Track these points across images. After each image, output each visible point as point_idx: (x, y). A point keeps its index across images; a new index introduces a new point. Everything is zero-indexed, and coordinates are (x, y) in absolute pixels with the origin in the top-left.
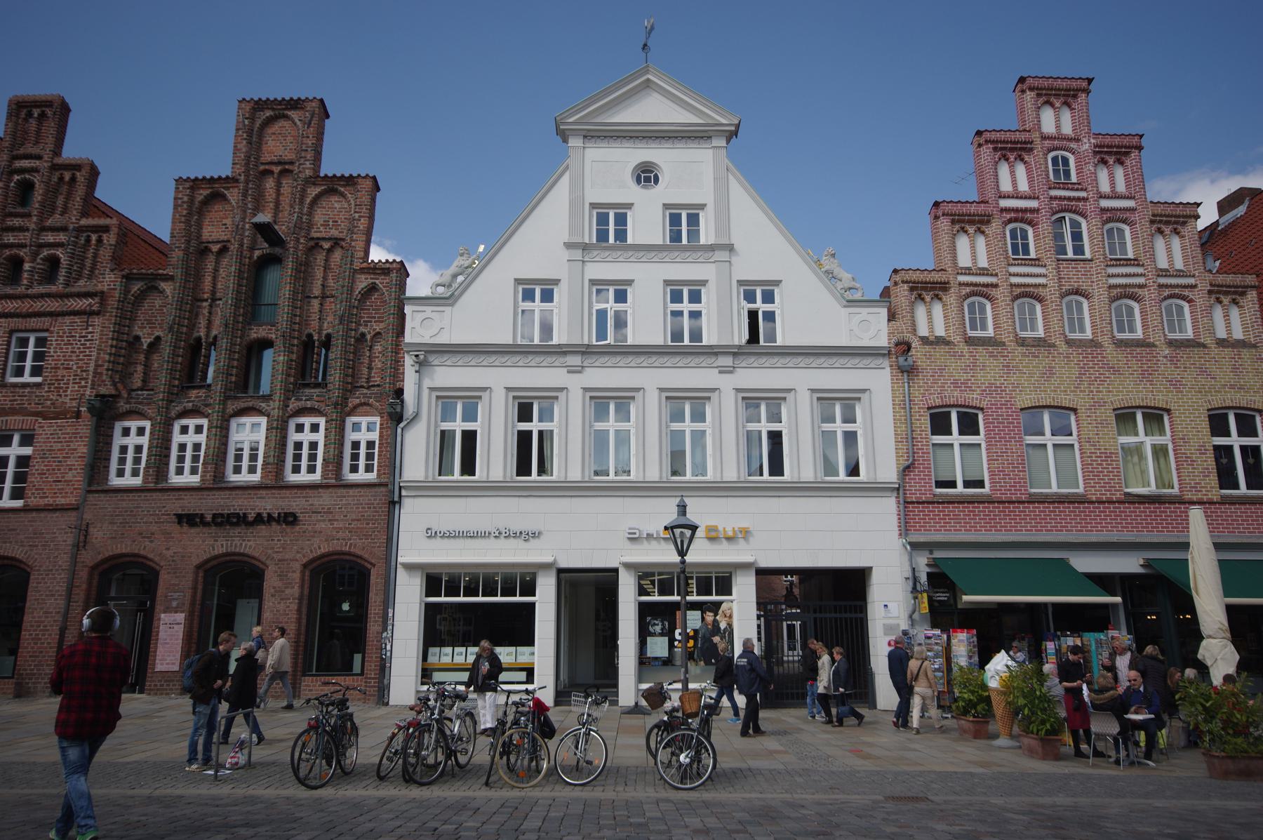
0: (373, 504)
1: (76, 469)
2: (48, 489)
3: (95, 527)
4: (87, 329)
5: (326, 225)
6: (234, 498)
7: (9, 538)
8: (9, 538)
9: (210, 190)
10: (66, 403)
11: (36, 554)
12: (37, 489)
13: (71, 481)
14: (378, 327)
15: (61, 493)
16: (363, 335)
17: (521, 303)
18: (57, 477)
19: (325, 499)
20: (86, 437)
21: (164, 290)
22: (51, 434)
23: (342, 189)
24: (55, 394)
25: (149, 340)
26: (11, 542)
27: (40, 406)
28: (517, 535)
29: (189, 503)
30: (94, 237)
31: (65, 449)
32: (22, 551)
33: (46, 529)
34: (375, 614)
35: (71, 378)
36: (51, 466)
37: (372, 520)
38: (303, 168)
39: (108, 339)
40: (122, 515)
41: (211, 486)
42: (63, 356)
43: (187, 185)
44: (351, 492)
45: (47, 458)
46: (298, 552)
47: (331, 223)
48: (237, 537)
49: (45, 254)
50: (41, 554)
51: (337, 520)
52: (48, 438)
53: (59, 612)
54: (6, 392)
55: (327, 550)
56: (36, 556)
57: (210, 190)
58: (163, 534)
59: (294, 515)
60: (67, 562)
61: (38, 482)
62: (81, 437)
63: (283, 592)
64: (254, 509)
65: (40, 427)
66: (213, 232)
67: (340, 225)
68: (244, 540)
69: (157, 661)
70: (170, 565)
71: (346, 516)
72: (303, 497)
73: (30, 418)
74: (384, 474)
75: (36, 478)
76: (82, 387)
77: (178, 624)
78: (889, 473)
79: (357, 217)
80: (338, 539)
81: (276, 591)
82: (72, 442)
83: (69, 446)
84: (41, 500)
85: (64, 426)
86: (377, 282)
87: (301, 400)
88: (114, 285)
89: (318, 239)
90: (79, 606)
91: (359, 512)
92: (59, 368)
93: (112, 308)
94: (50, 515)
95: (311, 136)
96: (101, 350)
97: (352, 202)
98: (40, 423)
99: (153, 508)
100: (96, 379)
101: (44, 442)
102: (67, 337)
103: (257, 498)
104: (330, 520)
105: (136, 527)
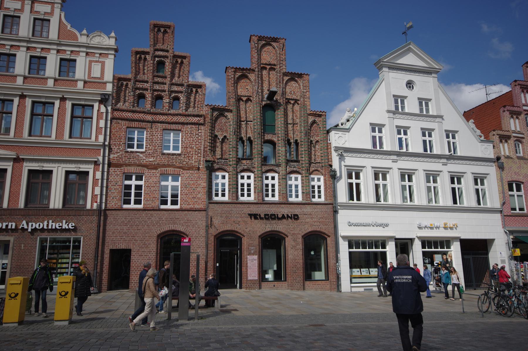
0: (327, 212)
1: (202, 193)
2: (190, 201)
3: (214, 218)
5: (291, 93)
6: (271, 208)
7: (176, 222)
8: (176, 222)
9: (241, 73)
11: (190, 229)
12: (185, 201)
13: (200, 198)
14: (317, 138)
15: (196, 203)
16: (311, 141)
17: (372, 133)
18: (194, 196)
19: (308, 209)
20: (204, 179)
21: (227, 116)
22: (188, 177)
23: (297, 79)
24: (187, 159)
25: (222, 137)
26: (177, 224)
27: (181, 164)
28: (381, 225)
29: (253, 209)
30: (194, 90)
34: (332, 256)
35: (194, 152)
36: (190, 191)
37: (327, 218)
38: (282, 68)
40: (225, 214)
41: (262, 202)
42: (189, 142)
43: (233, 70)
44: (318, 206)
45: (188, 187)
46: (300, 231)
47: (292, 92)
48: (275, 224)
49: (174, 95)
51: (314, 218)
52: (187, 179)
53: (203, 255)
54: (165, 157)
55: (311, 230)
57: (241, 73)
58: (244, 222)
59: (297, 215)
60: (204, 233)
61: (185, 198)
62: (202, 179)
63: (296, 247)
64: (280, 213)
65: (182, 173)
66: (242, 91)
67: (296, 94)
68: (278, 225)
69: (248, 276)
70: (248, 235)
71: (317, 216)
72: (299, 208)
73: (177, 169)
74: (330, 199)
75: (184, 196)
76: (199, 157)
77: (255, 260)
78: (497, 205)
79: (305, 91)
80: (315, 226)
81: (293, 247)
82: (198, 181)
84: (188, 206)
85: (193, 174)
86: (316, 119)
87: (292, 167)
88: (208, 112)
89: (289, 99)
90: (212, 252)
91: (322, 215)
93: (208, 122)
94: (193, 212)
95: (284, 55)
96: (205, 140)
97: (301, 84)
98: (182, 172)
99: (238, 211)
101: (185, 180)
102: (190, 134)
103: (281, 208)
104: (311, 218)
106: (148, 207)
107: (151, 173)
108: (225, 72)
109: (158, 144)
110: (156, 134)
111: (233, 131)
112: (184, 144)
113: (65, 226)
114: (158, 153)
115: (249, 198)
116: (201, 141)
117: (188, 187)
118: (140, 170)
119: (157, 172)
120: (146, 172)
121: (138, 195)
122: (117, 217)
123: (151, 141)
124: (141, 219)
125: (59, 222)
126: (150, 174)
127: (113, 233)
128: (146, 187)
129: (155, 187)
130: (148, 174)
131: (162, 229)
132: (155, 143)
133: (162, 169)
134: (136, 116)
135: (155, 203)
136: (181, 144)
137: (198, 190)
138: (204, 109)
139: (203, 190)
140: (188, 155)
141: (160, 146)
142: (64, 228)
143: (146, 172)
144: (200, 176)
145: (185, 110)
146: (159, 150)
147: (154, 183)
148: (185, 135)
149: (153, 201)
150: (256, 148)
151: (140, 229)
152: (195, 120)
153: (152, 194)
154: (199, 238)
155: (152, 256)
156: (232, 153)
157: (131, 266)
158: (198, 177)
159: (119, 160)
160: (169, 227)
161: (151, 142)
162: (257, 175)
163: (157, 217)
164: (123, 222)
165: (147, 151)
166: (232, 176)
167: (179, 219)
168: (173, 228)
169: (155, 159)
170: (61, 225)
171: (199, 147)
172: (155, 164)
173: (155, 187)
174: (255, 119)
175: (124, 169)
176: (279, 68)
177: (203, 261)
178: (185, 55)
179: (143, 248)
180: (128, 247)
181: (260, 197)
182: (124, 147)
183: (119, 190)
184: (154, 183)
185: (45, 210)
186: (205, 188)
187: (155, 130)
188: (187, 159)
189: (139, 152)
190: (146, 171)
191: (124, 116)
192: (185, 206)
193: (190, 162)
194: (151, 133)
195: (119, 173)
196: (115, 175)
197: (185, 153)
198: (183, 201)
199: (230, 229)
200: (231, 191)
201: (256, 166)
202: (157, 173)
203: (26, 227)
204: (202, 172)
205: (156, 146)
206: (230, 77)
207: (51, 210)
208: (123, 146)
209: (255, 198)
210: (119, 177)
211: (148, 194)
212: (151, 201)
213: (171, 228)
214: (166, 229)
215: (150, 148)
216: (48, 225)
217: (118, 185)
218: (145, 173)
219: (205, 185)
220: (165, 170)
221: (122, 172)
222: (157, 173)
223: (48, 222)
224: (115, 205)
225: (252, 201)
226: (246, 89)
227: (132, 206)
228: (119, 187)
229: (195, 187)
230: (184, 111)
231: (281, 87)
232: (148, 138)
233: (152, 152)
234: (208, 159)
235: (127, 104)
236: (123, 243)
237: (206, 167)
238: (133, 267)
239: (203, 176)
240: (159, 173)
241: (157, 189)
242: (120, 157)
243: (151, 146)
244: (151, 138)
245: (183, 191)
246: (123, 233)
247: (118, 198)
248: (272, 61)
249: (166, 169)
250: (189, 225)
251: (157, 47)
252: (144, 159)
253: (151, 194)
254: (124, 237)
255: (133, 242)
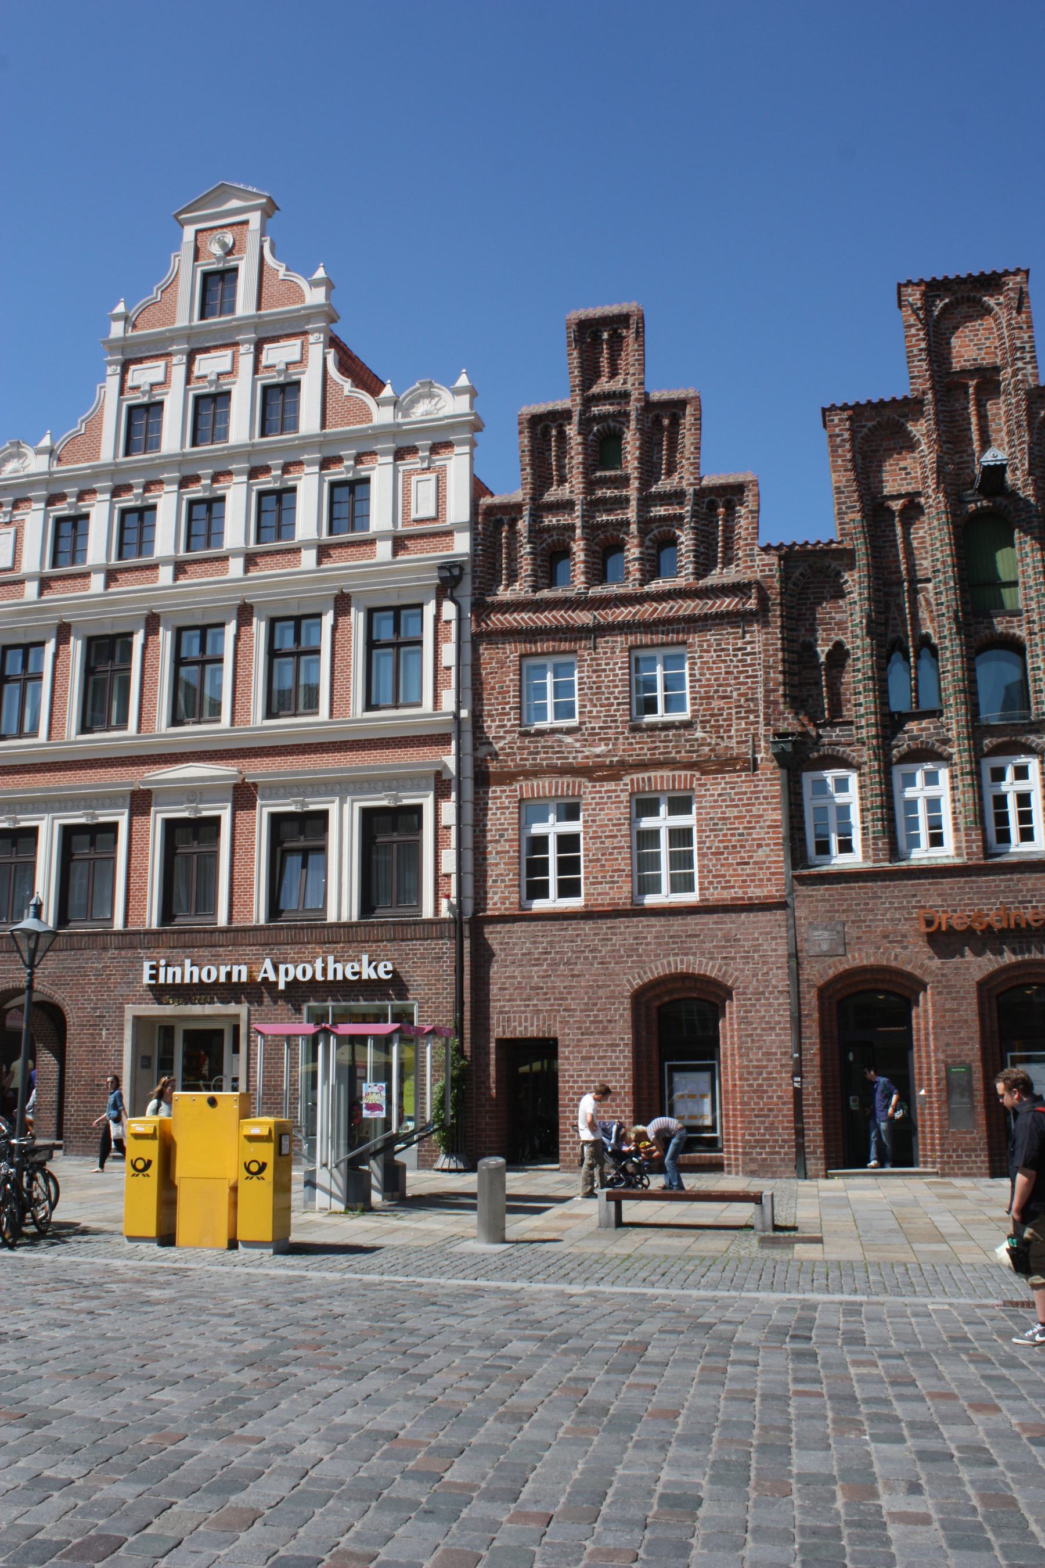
1: (768, 845)
4: (744, 637)
7: (691, 948)
10: (732, 748)
12: (714, 876)
13: (764, 863)
15: (752, 881)
18: (742, 858)
20: (773, 797)
22: (720, 795)
24: (714, 736)
25: (827, 649)
26: (694, 954)
27: (695, 755)
31: (745, 817)
32: (713, 967)
33: (742, 934)
35: (734, 711)
36: (730, 841)
39: (776, 650)
42: (716, 680)
43: (845, 415)
45: (721, 830)
50: (742, 970)
52: (716, 801)
54: (641, 737)
56: (736, 973)
60: (784, 980)
61: (713, 866)
65: (700, 785)
70: (939, 981)
73: (683, 773)
75: (711, 860)
76: (752, 723)
82: (753, 805)
83: (751, 811)
84: (725, 892)
85: (737, 782)
90: (814, 1044)
92: (712, 697)
95: (1025, 326)
96: (769, 667)
99: (897, 897)
100: (770, 711)
101: (712, 807)
102: (715, 651)
105: (877, 927)
106: (600, 902)
107: (600, 792)
108: (825, 426)
109: (616, 698)
110: (607, 664)
111: (861, 622)
112: (701, 686)
113: (368, 973)
114: (617, 727)
115: (936, 851)
116: (753, 671)
117: (721, 830)
118: (568, 786)
119: (622, 789)
120: (587, 791)
121: (569, 865)
122: (510, 938)
123: (595, 691)
124: (582, 941)
125: (353, 961)
126: (601, 798)
127: (500, 989)
128: (591, 838)
129: (615, 836)
130: (593, 798)
131: (645, 973)
132: (609, 693)
133: (635, 776)
134: (546, 619)
135: (621, 887)
136: (691, 687)
137: (754, 836)
138: (758, 562)
139: (771, 835)
140: (717, 721)
141: (624, 704)
142: (365, 977)
143: (587, 791)
144: (760, 788)
145: (693, 574)
146: (621, 716)
147: (614, 825)
148: (701, 657)
149: (613, 882)
150: (948, 671)
151: (579, 976)
152: (727, 604)
153: (610, 860)
154: (768, 999)
155: (622, 1060)
156: (865, 697)
157: (561, 1091)
158: (752, 793)
159: (506, 761)
160: (669, 964)
161: (597, 693)
162: (958, 767)
163: (630, 933)
164: (529, 954)
165: (584, 723)
166: (871, 779)
167: (698, 936)
168: (682, 968)
169: (610, 747)
170: (357, 969)
171: (750, 692)
172: (611, 762)
173: (615, 836)
174: (938, 571)
175: (521, 787)
176: (1012, 377)
177: (786, 1072)
178: (682, 396)
179: (592, 1033)
180: (549, 1032)
181: (974, 845)
182: (515, 719)
183: (512, 854)
184: (614, 825)
185: (316, 927)
186: (777, 827)
187: (605, 653)
188: (714, 736)
189: (562, 729)
190: (586, 787)
191: (509, 622)
192: (717, 895)
193: (723, 745)
194: (594, 663)
195: (507, 801)
196: (497, 809)
197: (704, 716)
198: (707, 877)
199: (872, 961)
200: (871, 830)
201: (952, 734)
202: (622, 791)
203: (272, 978)
204: (765, 774)
205: (612, 705)
206: (838, 439)
207: (331, 926)
208: (512, 716)
209: (958, 848)
210: (507, 815)
211: (598, 860)
212: (607, 883)
213: (676, 968)
214: (660, 969)
215: (594, 714)
216: (325, 970)
217: (506, 841)
218: (585, 793)
219: (779, 817)
220: (643, 779)
221: (516, 796)
222: (622, 791)
223: (325, 961)
224: (503, 903)
225: (946, 861)
226: (900, 469)
227: (552, 902)
228: (511, 846)
229: (745, 828)
230: (691, 577)
231: (1023, 442)
232: (585, 683)
233: (601, 725)
234: (783, 727)
235: (517, 586)
236: (532, 1018)
237: (776, 755)
238: (567, 1093)
239: (769, 788)
240: (627, 790)
241: (623, 844)
242: (508, 751)
243: (595, 706)
244: (594, 679)
245: (704, 842)
246: (532, 988)
247: (510, 880)
248: (983, 359)
249: (646, 775)
250: (733, 955)
251: (595, 390)
252: (577, 752)
253: (606, 860)
254: (535, 1002)
255: (561, 1016)
